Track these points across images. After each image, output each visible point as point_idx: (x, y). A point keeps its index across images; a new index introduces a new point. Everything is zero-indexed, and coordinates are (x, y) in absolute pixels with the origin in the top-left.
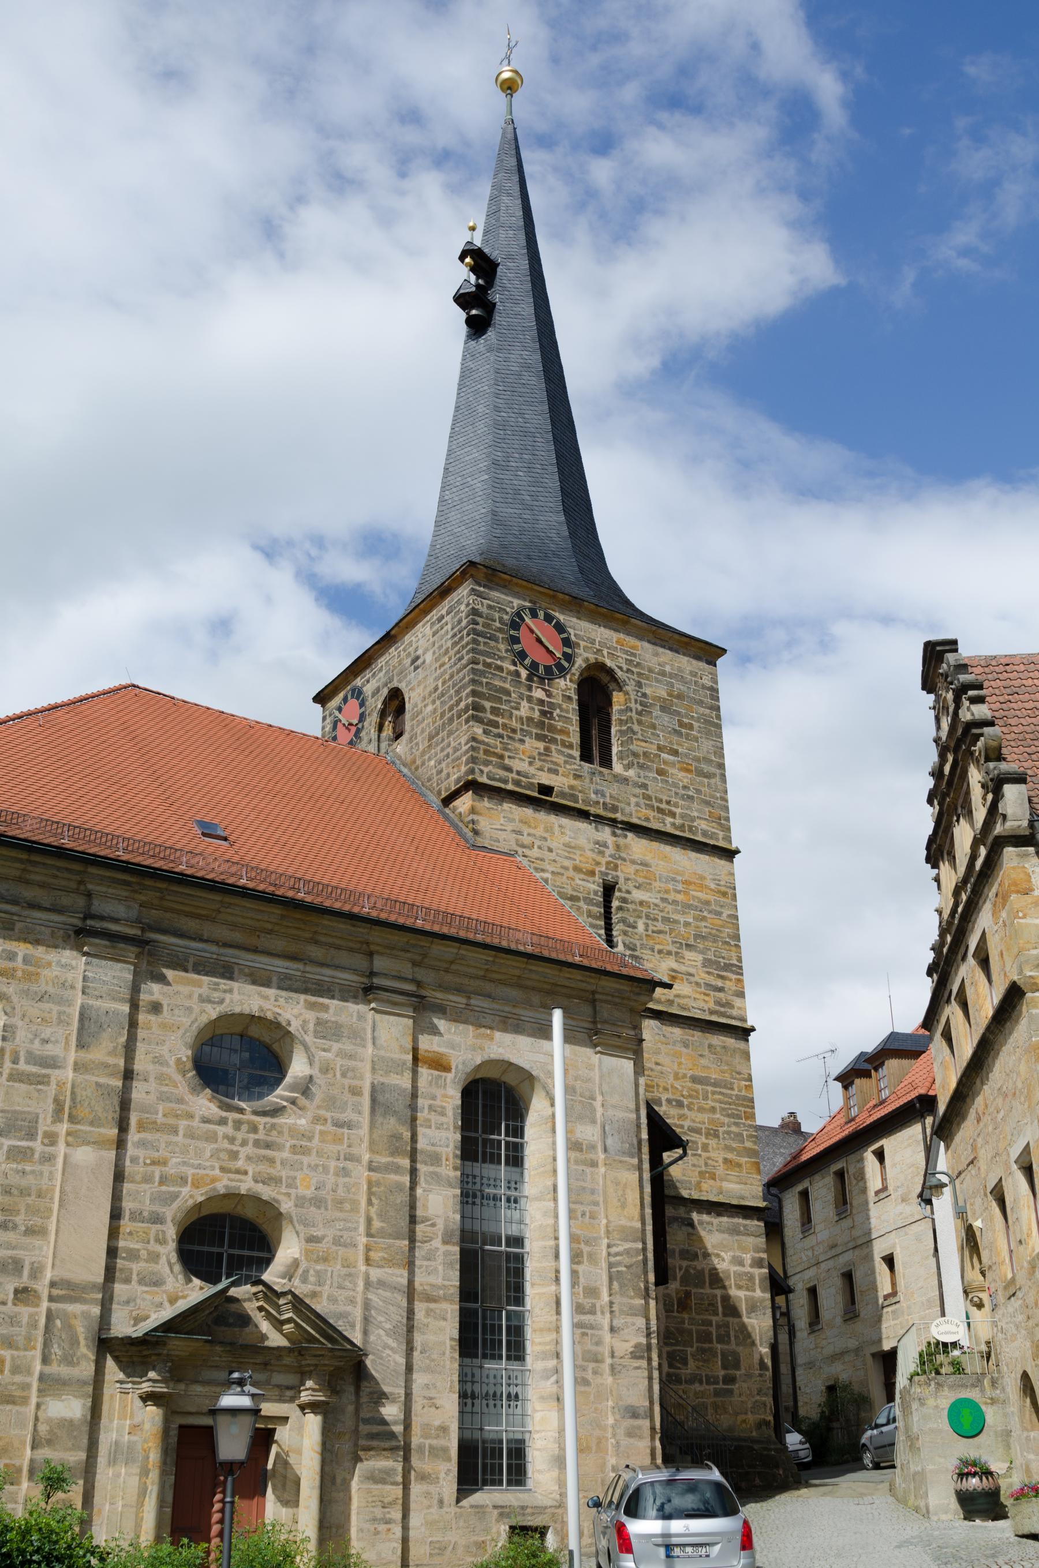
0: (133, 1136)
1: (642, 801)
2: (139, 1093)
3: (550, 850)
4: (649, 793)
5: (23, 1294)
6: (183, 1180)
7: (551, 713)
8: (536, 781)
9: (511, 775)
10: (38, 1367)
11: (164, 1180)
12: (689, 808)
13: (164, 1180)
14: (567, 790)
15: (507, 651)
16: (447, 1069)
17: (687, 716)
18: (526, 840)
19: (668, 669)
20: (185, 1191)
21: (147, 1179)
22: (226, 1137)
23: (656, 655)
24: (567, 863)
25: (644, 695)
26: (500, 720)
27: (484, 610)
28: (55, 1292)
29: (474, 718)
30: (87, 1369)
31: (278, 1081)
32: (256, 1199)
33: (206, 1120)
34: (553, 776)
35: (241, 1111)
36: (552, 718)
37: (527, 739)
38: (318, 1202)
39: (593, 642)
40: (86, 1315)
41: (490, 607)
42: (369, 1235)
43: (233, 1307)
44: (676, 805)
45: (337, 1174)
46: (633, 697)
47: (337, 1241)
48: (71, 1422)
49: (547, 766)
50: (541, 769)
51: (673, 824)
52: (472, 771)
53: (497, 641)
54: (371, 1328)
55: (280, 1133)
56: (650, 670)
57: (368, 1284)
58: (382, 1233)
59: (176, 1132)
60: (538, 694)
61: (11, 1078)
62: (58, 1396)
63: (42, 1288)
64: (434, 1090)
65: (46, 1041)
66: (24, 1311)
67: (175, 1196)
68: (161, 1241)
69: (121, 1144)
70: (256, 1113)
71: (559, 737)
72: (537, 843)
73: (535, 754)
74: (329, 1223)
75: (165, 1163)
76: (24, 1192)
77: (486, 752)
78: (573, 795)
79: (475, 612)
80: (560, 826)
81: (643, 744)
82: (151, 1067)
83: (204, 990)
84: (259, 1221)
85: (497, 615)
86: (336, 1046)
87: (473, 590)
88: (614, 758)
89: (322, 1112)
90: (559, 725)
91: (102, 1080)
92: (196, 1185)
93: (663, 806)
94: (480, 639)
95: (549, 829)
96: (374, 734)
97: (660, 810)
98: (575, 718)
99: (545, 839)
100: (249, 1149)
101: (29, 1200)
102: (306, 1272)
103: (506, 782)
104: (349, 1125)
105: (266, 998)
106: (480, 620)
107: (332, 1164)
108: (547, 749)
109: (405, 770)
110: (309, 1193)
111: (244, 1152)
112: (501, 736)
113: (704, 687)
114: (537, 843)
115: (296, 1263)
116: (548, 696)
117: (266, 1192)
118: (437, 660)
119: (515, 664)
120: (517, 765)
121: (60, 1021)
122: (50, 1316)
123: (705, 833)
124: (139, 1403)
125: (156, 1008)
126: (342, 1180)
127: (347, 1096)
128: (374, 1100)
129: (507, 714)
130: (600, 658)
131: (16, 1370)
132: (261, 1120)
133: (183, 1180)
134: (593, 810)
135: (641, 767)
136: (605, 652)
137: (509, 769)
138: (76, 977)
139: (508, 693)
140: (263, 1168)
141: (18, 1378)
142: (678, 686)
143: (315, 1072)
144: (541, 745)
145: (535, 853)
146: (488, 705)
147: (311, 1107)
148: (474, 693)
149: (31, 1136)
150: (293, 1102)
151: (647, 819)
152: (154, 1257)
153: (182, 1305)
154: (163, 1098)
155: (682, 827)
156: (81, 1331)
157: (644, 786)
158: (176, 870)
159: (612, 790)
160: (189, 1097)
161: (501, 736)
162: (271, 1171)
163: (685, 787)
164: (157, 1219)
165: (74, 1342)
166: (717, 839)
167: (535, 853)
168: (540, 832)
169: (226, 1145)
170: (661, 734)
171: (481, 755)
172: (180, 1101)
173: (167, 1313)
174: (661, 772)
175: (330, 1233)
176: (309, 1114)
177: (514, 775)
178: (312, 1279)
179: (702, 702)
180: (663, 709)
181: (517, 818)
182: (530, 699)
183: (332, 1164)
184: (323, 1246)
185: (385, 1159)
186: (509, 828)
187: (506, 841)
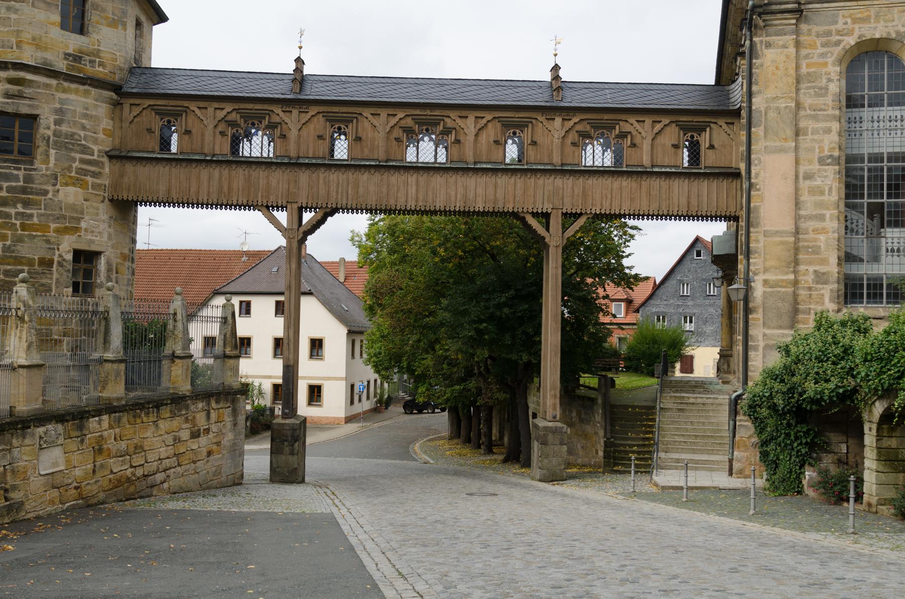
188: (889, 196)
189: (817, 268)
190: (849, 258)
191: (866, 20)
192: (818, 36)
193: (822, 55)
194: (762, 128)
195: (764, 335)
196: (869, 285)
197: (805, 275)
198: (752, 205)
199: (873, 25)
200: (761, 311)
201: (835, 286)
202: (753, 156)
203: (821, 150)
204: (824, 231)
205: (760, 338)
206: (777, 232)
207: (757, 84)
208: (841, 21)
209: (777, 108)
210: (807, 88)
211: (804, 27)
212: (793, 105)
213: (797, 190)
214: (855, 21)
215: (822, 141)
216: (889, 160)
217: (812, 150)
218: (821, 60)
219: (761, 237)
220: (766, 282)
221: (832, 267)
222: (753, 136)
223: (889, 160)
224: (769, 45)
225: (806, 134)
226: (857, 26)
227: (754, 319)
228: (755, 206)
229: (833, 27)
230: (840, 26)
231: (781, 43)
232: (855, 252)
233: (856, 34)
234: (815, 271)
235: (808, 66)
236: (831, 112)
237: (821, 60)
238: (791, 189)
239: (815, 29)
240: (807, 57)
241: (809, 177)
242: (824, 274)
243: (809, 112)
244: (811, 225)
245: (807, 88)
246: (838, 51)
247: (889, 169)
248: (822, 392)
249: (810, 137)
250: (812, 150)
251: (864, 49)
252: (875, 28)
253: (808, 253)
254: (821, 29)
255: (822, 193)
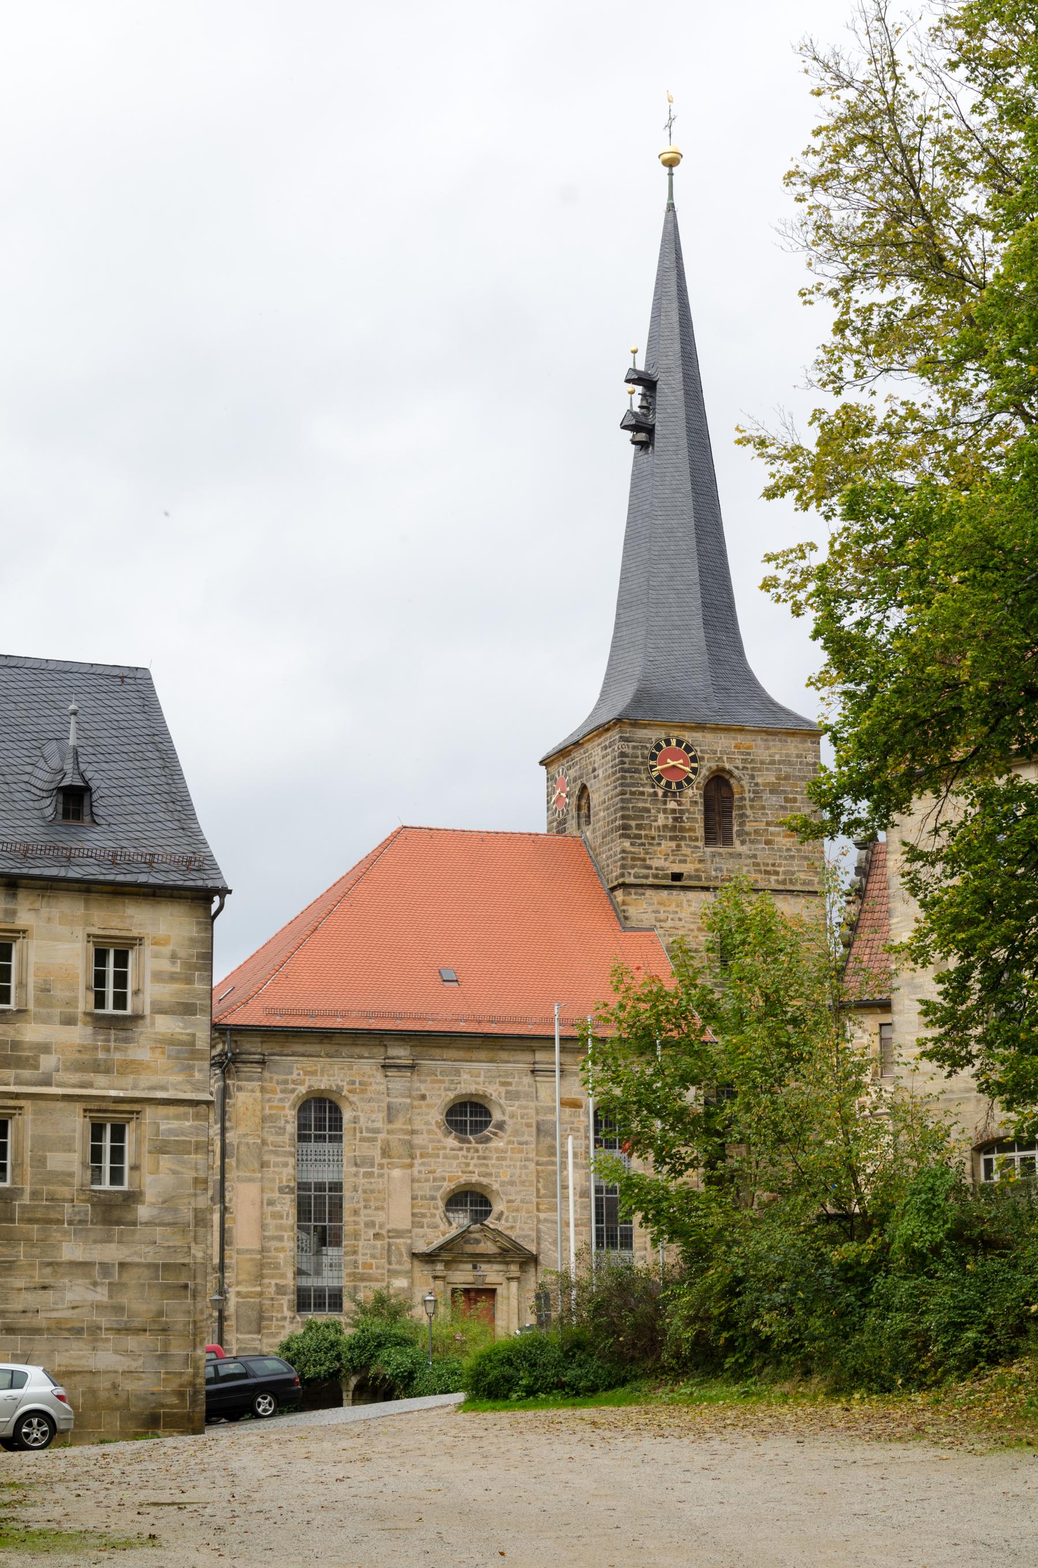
0: (418, 1161)
1: (752, 868)
2: (418, 1140)
3: (680, 920)
4: (758, 861)
5: (377, 1236)
6: (444, 1179)
7: (681, 818)
8: (669, 872)
9: (650, 871)
10: (387, 1266)
11: (435, 1180)
12: (791, 865)
13: (435, 1180)
14: (693, 873)
15: (647, 778)
16: (580, 1107)
17: (792, 792)
18: (662, 916)
19: (777, 758)
20: (445, 1184)
21: (427, 1180)
22: (463, 1156)
23: (768, 748)
24: (692, 926)
25: (757, 784)
26: (643, 833)
27: (629, 751)
28: (391, 1234)
29: (622, 836)
30: (407, 1266)
31: (487, 1124)
32: (480, 1184)
33: (452, 1149)
34: (683, 865)
35: (470, 1142)
36: (682, 821)
37: (663, 842)
38: (512, 1183)
39: (715, 752)
40: (405, 1244)
41: (634, 747)
42: (538, 1197)
43: (473, 1236)
44: (780, 865)
45: (521, 1169)
46: (746, 789)
47: (522, 1201)
48: (403, 1288)
49: (678, 858)
50: (674, 862)
51: (777, 881)
52: (622, 875)
53: (640, 773)
54: (541, 1242)
55: (490, 1151)
56: (762, 763)
57: (539, 1221)
58: (545, 1196)
59: (438, 1156)
60: (672, 805)
61: (361, 1140)
62: (397, 1278)
63: (384, 1232)
64: (572, 1119)
65: (373, 1121)
66: (379, 1243)
67: (440, 1187)
68: (436, 1208)
69: (411, 1166)
70: (477, 1143)
71: (687, 835)
72: (671, 916)
73: (669, 852)
74: (518, 1193)
75: (434, 1172)
76: (372, 1191)
77: (633, 859)
78: (697, 876)
79: (623, 755)
80: (688, 901)
81: (754, 824)
82: (424, 1127)
83: (447, 1085)
84: (484, 1193)
85: (639, 752)
86: (517, 1103)
87: (621, 737)
88: (735, 835)
89: (512, 1138)
90: (687, 825)
91: (401, 1137)
92: (450, 1181)
93: (769, 868)
94: (627, 774)
95: (679, 905)
96: (574, 813)
97: (767, 872)
98: (700, 816)
99: (677, 912)
100: (475, 1161)
101: (375, 1195)
102: (507, 1217)
103: (646, 877)
104: (526, 1143)
105: (479, 1084)
106: (626, 760)
107: (518, 1164)
108: (678, 846)
109: (591, 853)
110: (507, 1179)
111: (472, 1162)
112: (643, 844)
113: (808, 764)
114: (671, 916)
115: (502, 1213)
116: (679, 805)
117: (485, 1181)
118: (605, 778)
119: (653, 787)
120: (655, 863)
121: (379, 1111)
122: (389, 1245)
123: (804, 883)
124: (431, 1280)
125: (423, 1097)
126: (524, 1171)
127: (525, 1129)
128: (538, 1130)
129: (648, 827)
130: (720, 764)
131: (377, 1268)
132: (480, 1146)
133: (444, 1179)
134: (712, 884)
135: (752, 842)
136: (725, 759)
137: (650, 868)
138: (382, 1088)
139: (648, 810)
140: (482, 1169)
141: (379, 1271)
142: (785, 769)
143: (506, 1118)
144: (673, 844)
145: (669, 924)
146: (633, 823)
147: (506, 1136)
148: (623, 817)
149: (372, 1166)
150: (495, 1134)
151: (756, 881)
152: (433, 1216)
153: (448, 1237)
154: (431, 1141)
155: (784, 882)
156: (404, 1250)
157: (755, 856)
158: (426, 1029)
159: (727, 865)
160: (443, 1139)
161: (643, 844)
162: (488, 1171)
163: (788, 850)
164: (433, 1198)
165: (401, 1255)
166: (813, 884)
167: (669, 924)
168: (673, 908)
169: (464, 1160)
170: (769, 812)
171: (629, 862)
172: (439, 1141)
173: (437, 1243)
174: (768, 842)
175: (519, 1198)
176: (505, 1140)
177: (654, 871)
178: (511, 1220)
179: (805, 777)
180: (772, 792)
181: (656, 902)
182: (665, 811)
183: (518, 1164)
184: (515, 1204)
185: (545, 1159)
186: (650, 910)
187: (648, 919)
188: (330, 1221)
189: (278, 1281)
190: (300, 1272)
191: (313, 1073)
192: (278, 1083)
193: (281, 1100)
194: (234, 1159)
195: (238, 1339)
196: (330, 1296)
197: (268, 1287)
198: (226, 1226)
199: (319, 1078)
200: (234, 1318)
201: (292, 1297)
202: (227, 1184)
203: (281, 1181)
204: (282, 1249)
205: (234, 1342)
206: (247, 1250)
207: (230, 1120)
208: (295, 1072)
209: (247, 1144)
210: (270, 1127)
211: (267, 1075)
212: (259, 1141)
213: (262, 1214)
214: (306, 1073)
215: (281, 1173)
216: (330, 1190)
217: (273, 1180)
218: (280, 1104)
219: (235, 1255)
220: (238, 1294)
221: (289, 1281)
222: (226, 1166)
223: (330, 1190)
224: (240, 1089)
225: (268, 1167)
226: (307, 1078)
227: (228, 1326)
228: (229, 1228)
229: (289, 1077)
230: (294, 1076)
231: (250, 1088)
232: (304, 1267)
233: (307, 1084)
234: (276, 1284)
235: (270, 1108)
236: (288, 1149)
237: (280, 1104)
238: (258, 1214)
239: (276, 1077)
240: (269, 1100)
241: (271, 1203)
242: (283, 1286)
243: (271, 1148)
244: (273, 1244)
245: (270, 1127)
246: (293, 1096)
247: (330, 1197)
248: (319, 1373)
249: (272, 1169)
250: (274, 1180)
251: (312, 1096)
252: (321, 1081)
253: (271, 1269)
254: (281, 1077)
255: (281, 1217)
